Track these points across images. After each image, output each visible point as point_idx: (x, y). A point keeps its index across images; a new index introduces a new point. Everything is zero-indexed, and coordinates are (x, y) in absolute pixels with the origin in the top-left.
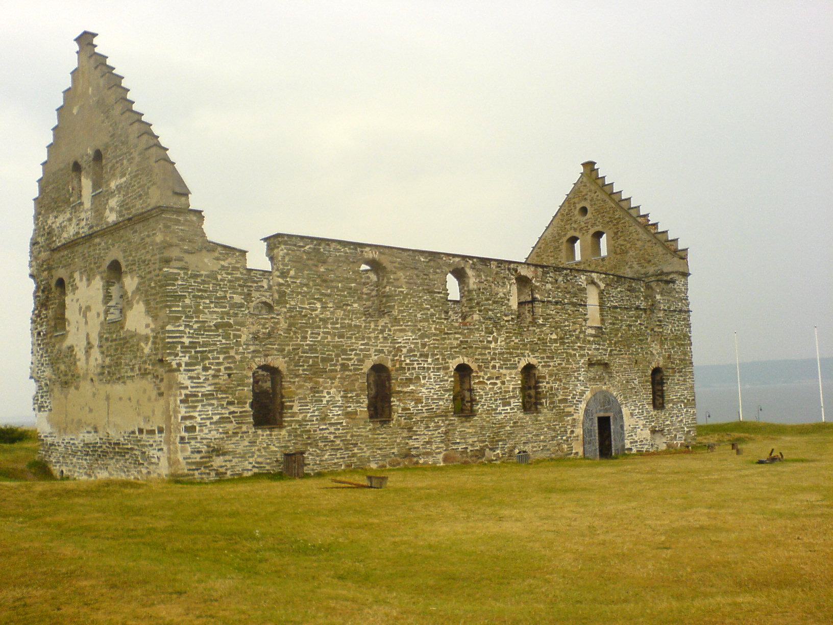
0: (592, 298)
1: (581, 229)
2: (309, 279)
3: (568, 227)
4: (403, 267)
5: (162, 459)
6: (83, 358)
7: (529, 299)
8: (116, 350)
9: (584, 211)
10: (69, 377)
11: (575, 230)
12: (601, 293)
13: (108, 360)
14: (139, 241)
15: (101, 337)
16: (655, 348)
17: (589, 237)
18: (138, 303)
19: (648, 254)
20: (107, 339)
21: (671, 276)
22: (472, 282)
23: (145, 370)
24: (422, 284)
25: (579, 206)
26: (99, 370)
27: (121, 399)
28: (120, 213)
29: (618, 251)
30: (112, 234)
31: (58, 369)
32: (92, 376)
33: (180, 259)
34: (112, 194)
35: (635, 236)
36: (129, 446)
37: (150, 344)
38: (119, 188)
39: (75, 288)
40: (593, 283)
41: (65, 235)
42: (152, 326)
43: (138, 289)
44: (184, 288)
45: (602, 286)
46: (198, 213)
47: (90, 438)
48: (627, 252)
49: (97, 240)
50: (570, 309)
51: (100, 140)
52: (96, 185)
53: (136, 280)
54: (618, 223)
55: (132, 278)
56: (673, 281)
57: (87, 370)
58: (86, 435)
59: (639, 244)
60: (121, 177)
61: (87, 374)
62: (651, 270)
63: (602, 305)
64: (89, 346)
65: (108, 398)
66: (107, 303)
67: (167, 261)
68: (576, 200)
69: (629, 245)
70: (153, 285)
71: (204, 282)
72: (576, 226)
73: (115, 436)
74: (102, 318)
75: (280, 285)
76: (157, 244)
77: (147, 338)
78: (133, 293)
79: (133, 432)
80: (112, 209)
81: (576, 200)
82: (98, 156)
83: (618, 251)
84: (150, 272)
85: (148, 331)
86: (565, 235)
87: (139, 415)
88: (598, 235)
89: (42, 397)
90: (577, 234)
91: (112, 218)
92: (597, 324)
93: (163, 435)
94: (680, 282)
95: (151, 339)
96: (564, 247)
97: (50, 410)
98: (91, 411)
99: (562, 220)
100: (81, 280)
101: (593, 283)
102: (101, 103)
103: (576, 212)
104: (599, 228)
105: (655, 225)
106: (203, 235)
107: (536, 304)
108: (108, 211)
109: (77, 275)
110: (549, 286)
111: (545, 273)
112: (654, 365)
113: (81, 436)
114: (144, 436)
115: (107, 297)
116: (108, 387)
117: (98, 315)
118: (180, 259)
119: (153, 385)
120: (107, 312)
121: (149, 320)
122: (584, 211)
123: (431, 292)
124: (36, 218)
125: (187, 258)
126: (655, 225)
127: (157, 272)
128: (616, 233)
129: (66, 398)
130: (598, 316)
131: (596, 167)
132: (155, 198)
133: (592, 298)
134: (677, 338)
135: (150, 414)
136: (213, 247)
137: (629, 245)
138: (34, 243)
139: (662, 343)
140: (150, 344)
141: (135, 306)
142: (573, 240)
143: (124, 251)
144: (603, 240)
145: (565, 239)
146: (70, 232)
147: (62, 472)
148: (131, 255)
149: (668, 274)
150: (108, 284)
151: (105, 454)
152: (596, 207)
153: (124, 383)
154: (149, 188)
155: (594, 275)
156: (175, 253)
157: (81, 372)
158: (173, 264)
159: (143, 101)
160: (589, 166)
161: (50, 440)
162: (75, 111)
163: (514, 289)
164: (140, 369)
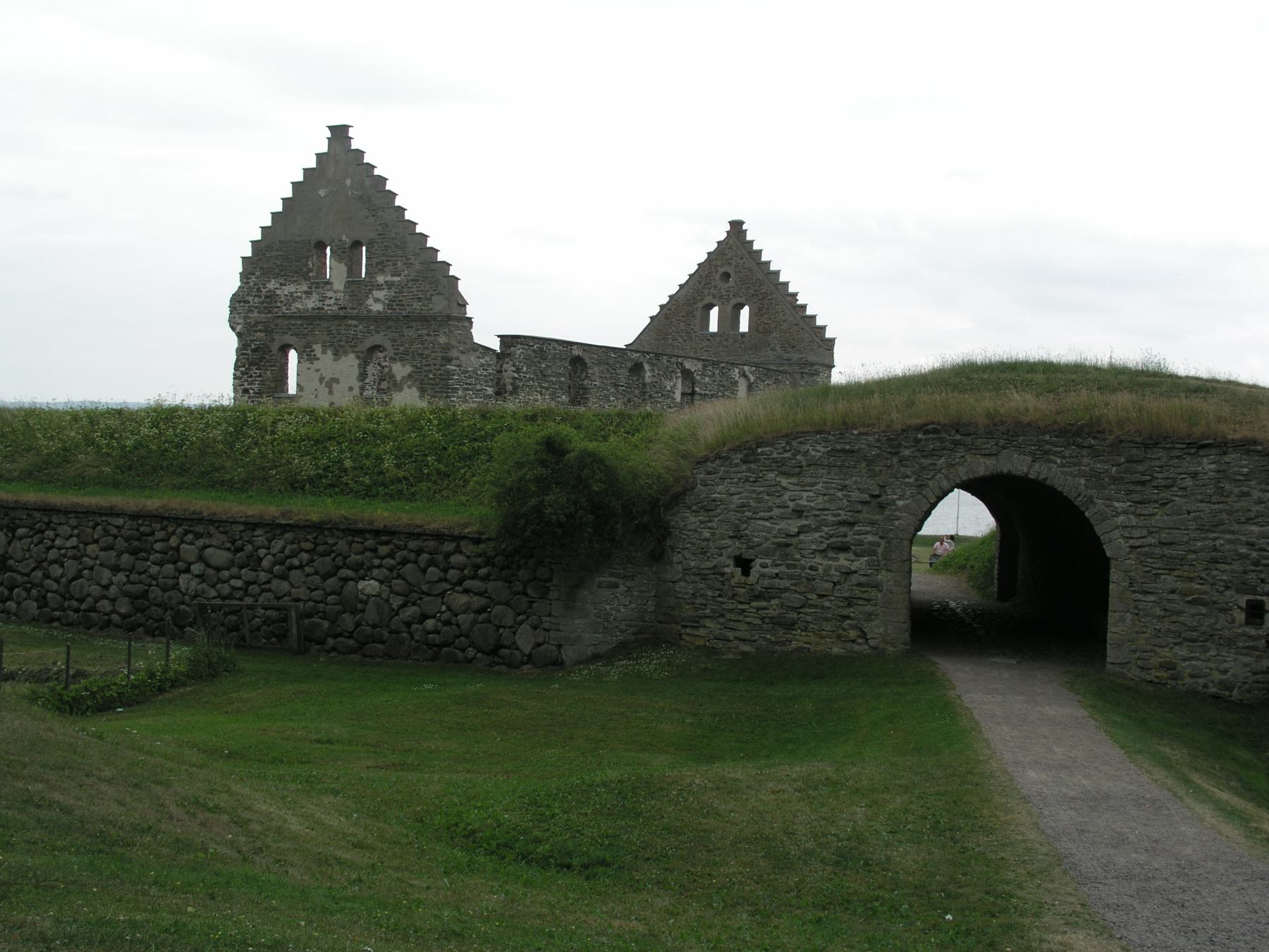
2: (535, 373)
3: (706, 291)
4: (599, 363)
7: (689, 391)
9: (726, 276)
11: (714, 296)
17: (729, 308)
18: (410, 387)
24: (611, 378)
25: (721, 270)
28: (389, 306)
29: (761, 329)
33: (457, 359)
34: (379, 287)
38: (389, 285)
40: (744, 375)
41: (300, 306)
43: (410, 376)
44: (458, 381)
45: (752, 379)
46: (470, 319)
48: (770, 332)
49: (354, 322)
53: (408, 369)
55: (403, 366)
56: (818, 374)
62: (795, 356)
66: (363, 380)
67: (449, 360)
68: (719, 263)
71: (470, 377)
74: (356, 391)
75: (514, 378)
78: (403, 378)
80: (377, 300)
81: (719, 263)
83: (761, 329)
90: (714, 302)
91: (377, 307)
96: (698, 314)
99: (700, 283)
100: (324, 352)
101: (744, 375)
103: (717, 277)
104: (742, 300)
105: (804, 307)
106: (471, 338)
107: (697, 397)
108: (370, 301)
109: (318, 348)
110: (707, 379)
111: (705, 366)
115: (363, 376)
117: (351, 389)
118: (457, 359)
120: (362, 389)
122: (726, 276)
123: (616, 386)
125: (462, 357)
126: (804, 307)
128: (760, 309)
131: (744, 227)
132: (438, 305)
141: (406, 390)
142: (711, 306)
143: (394, 340)
144: (745, 313)
145: (700, 305)
149: (812, 364)
150: (364, 364)
155: (746, 368)
156: (454, 353)
158: (454, 362)
162: (322, 193)
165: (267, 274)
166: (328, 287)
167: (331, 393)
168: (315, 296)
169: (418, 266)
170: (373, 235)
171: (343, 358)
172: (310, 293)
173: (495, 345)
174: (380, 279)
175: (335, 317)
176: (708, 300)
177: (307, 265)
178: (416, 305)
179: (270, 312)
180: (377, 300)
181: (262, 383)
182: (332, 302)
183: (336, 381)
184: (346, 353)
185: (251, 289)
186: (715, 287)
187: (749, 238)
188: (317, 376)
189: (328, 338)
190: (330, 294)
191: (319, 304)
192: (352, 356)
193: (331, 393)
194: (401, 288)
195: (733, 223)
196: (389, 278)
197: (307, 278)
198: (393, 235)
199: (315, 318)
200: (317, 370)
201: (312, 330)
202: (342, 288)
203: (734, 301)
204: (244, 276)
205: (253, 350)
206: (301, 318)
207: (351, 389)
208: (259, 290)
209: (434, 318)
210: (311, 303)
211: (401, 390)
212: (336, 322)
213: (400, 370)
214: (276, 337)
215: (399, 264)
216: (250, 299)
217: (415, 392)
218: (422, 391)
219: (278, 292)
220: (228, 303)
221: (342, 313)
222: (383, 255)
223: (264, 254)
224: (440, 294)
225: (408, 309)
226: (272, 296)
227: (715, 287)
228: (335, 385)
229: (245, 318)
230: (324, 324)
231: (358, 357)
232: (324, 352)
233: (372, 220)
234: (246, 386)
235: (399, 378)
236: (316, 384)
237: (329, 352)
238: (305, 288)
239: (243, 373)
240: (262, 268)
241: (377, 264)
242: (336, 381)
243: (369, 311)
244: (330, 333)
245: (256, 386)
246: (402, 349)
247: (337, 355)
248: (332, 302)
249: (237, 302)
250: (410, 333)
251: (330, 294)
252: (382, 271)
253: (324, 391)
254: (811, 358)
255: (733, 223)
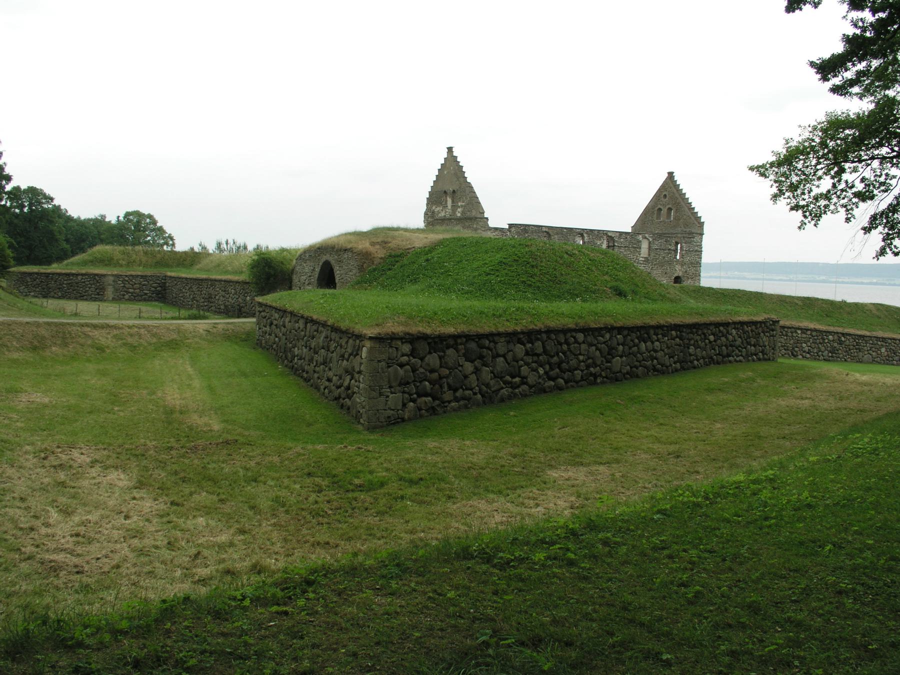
0: (645, 245)
4: (557, 234)
9: (665, 196)
12: (650, 243)
16: (678, 267)
22: (586, 238)
40: (646, 238)
50: (632, 249)
51: (455, 187)
52: (453, 202)
62: (688, 230)
63: (650, 247)
82: (454, 191)
88: (670, 209)
91: (459, 215)
92: (646, 256)
94: (697, 239)
101: (646, 238)
102: (455, 174)
112: (676, 275)
122: (665, 196)
124: (427, 205)
130: (647, 251)
132: (474, 213)
133: (645, 245)
134: (692, 263)
136: (490, 229)
138: (426, 214)
139: (682, 265)
146: (443, 214)
159: (470, 177)
160: (671, 175)
163: (605, 242)
173: (507, 227)
254: (693, 231)
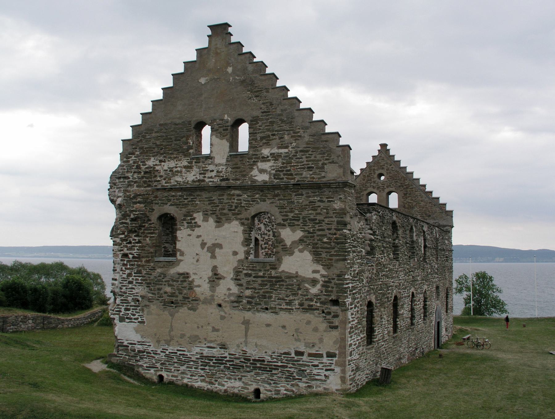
1: (378, 188)
3: (368, 185)
5: (331, 378)
6: (206, 286)
8: (262, 285)
10: (180, 297)
11: (374, 187)
13: (248, 293)
14: (307, 203)
15: (237, 272)
17: (384, 194)
18: (301, 251)
19: (429, 211)
20: (247, 275)
21: (447, 228)
23: (312, 306)
26: (232, 298)
27: (268, 325)
28: (276, 176)
29: (406, 206)
30: (262, 191)
31: (160, 289)
32: (220, 302)
34: (265, 159)
35: (420, 198)
36: (280, 364)
37: (319, 286)
38: (275, 157)
39: (193, 225)
41: (179, 179)
42: (324, 272)
43: (301, 240)
47: (216, 352)
49: (237, 192)
53: (299, 234)
54: (407, 188)
55: (293, 231)
57: (212, 296)
58: (207, 349)
59: (422, 204)
60: (279, 148)
61: (214, 299)
64: (216, 278)
65: (246, 323)
66: (248, 245)
69: (414, 203)
70: (325, 240)
72: (375, 185)
73: (253, 353)
75: (371, 240)
76: (335, 209)
77: (314, 282)
78: (293, 243)
79: (285, 353)
80: (262, 171)
84: (323, 230)
85: (317, 276)
86: (365, 190)
87: (298, 340)
89: (127, 309)
93: (334, 359)
95: (321, 283)
97: (142, 322)
98: (215, 330)
108: (255, 172)
109: (199, 217)
113: (198, 350)
114: (305, 358)
116: (248, 315)
119: (321, 319)
121: (320, 268)
127: (333, 231)
128: (405, 194)
129: (172, 315)
131: (388, 148)
135: (317, 341)
137: (414, 203)
140: (319, 286)
143: (281, 207)
147: (161, 377)
148: (291, 212)
151: (237, 367)
152: (391, 175)
153: (276, 313)
154: (324, 164)
157: (202, 298)
160: (384, 146)
161: (140, 347)
164: (301, 304)
165: (147, 152)
166: (210, 161)
167: (213, 257)
168: (195, 170)
169: (307, 138)
170: (257, 113)
171: (226, 225)
172: (191, 167)
174: (266, 152)
175: (217, 188)
176: (370, 189)
177: (187, 143)
178: (306, 174)
179: (149, 186)
180: (262, 171)
181: (142, 248)
182: (213, 174)
183: (220, 246)
184: (229, 220)
185: (131, 167)
186: (374, 182)
187: (391, 154)
188: (199, 241)
189: (209, 207)
190: (211, 167)
191: (201, 177)
192: (235, 223)
193: (213, 257)
194: (288, 159)
195: (382, 145)
196: (275, 150)
197: (186, 154)
198: (279, 112)
199: (197, 189)
200: (198, 237)
201: (225, 196)
202: (224, 161)
203: (387, 190)
204: (125, 156)
205: (132, 220)
206: (181, 189)
207: (235, 253)
208: (138, 167)
209: (328, 185)
210: (191, 176)
211: (291, 254)
212: (218, 193)
213: (289, 235)
214: (156, 207)
215: (286, 137)
216: (130, 175)
217: (307, 256)
218: (317, 257)
219: (157, 168)
220: (109, 180)
221: (224, 184)
222: (268, 130)
223: (144, 137)
224: (333, 162)
225: (297, 178)
226: (151, 172)
227: (374, 182)
228: (217, 250)
229: (125, 191)
230: (205, 195)
231: (243, 224)
232: (205, 220)
233: (255, 100)
234: (126, 251)
235: (288, 243)
236: (198, 249)
237: (211, 220)
238: (186, 164)
239: (122, 240)
240: (141, 148)
241: (262, 138)
242: (220, 246)
243: (256, 181)
244: (211, 202)
245: (135, 252)
246: (291, 215)
247: (219, 222)
248: (213, 174)
249: (117, 178)
250: (302, 200)
251: (211, 167)
252: (268, 144)
253: (205, 255)
255: (382, 145)
